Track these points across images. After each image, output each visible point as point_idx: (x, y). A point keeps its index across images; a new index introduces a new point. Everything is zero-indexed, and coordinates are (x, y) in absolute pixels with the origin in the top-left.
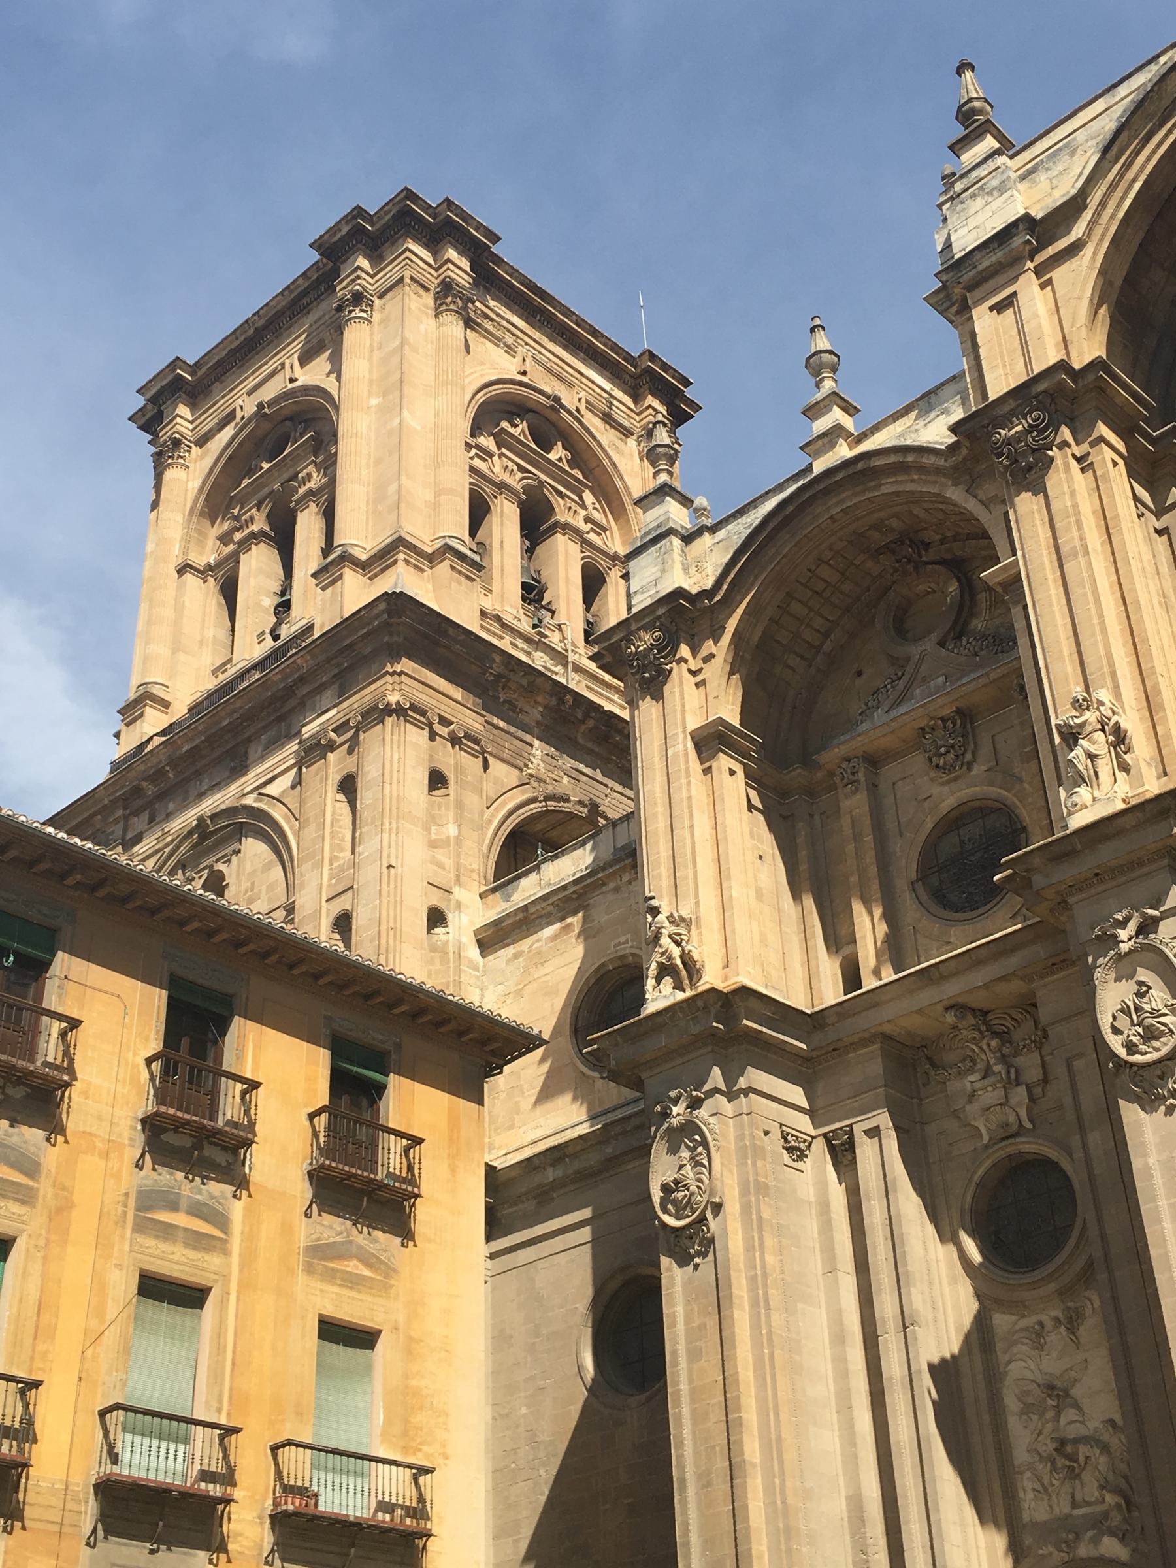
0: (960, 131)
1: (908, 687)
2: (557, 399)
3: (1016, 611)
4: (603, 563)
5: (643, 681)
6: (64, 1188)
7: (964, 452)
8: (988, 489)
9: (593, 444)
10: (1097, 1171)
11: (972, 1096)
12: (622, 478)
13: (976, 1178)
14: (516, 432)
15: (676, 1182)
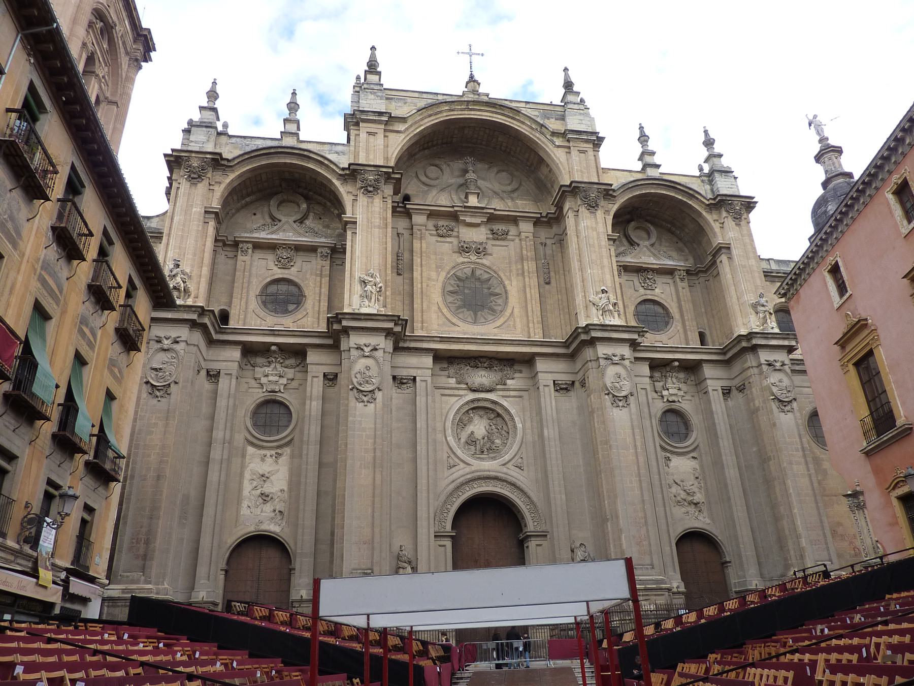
0: (367, 69)
1: (277, 230)
2: (115, 25)
3: (349, 233)
4: (102, 98)
5: (190, 176)
6: (66, 303)
7: (348, 172)
8: (349, 188)
9: (118, 49)
10: (312, 414)
11: (267, 376)
12: (122, 70)
13: (259, 401)
14: (97, 26)
15: (160, 369)
